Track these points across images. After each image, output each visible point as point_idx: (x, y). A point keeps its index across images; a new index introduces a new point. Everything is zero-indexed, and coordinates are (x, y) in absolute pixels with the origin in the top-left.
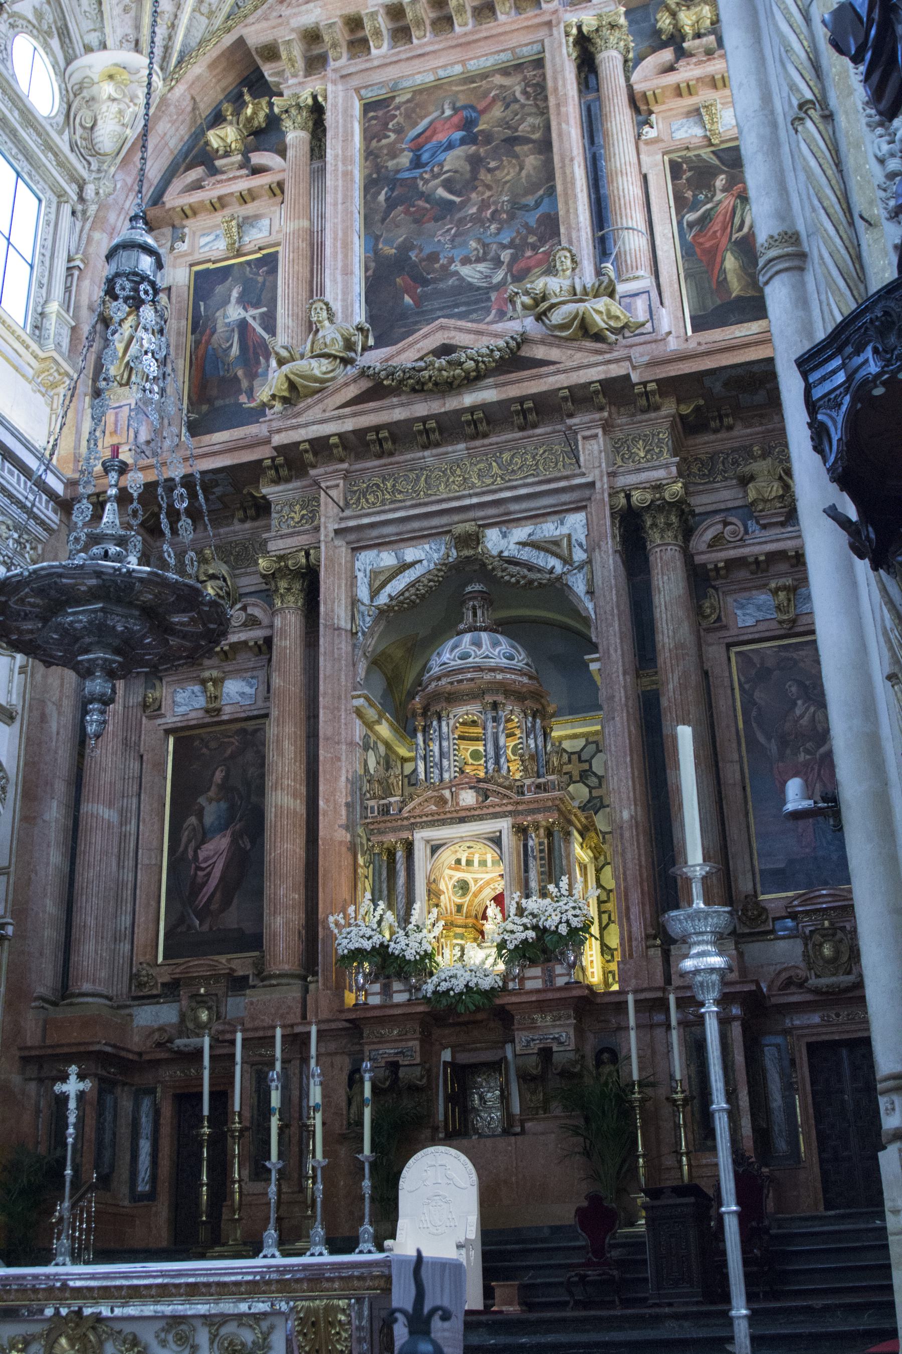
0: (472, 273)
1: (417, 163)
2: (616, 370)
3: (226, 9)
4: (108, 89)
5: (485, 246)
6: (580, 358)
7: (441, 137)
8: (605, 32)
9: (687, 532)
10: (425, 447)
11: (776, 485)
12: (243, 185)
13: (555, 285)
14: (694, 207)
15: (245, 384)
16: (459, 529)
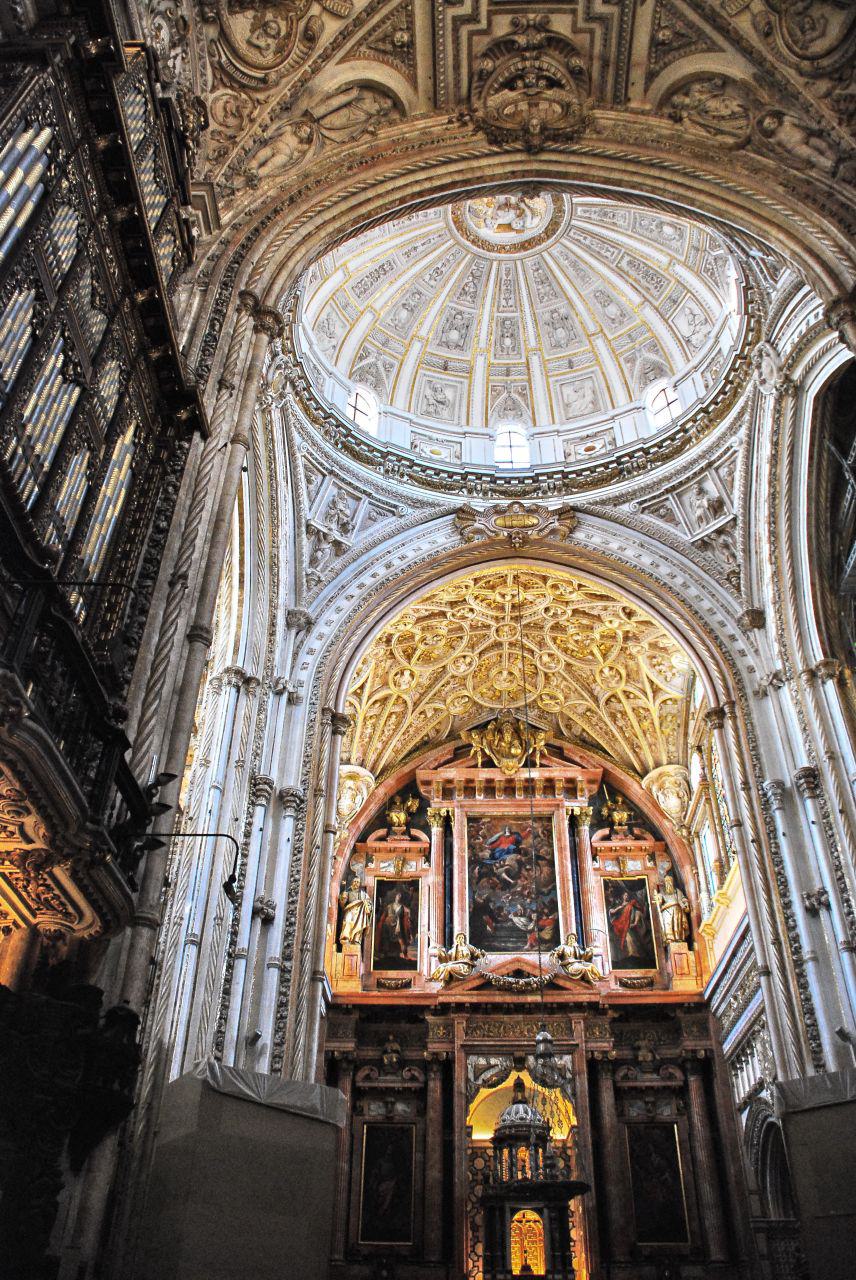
0: (519, 921)
1: (493, 857)
2: (594, 999)
3: (405, 752)
4: (350, 783)
5: (525, 909)
6: (579, 989)
7: (504, 846)
8: (584, 818)
9: (614, 1072)
10: (506, 1013)
11: (650, 1055)
12: (406, 845)
13: (569, 950)
14: (614, 906)
15: (403, 947)
16: (518, 1054)
